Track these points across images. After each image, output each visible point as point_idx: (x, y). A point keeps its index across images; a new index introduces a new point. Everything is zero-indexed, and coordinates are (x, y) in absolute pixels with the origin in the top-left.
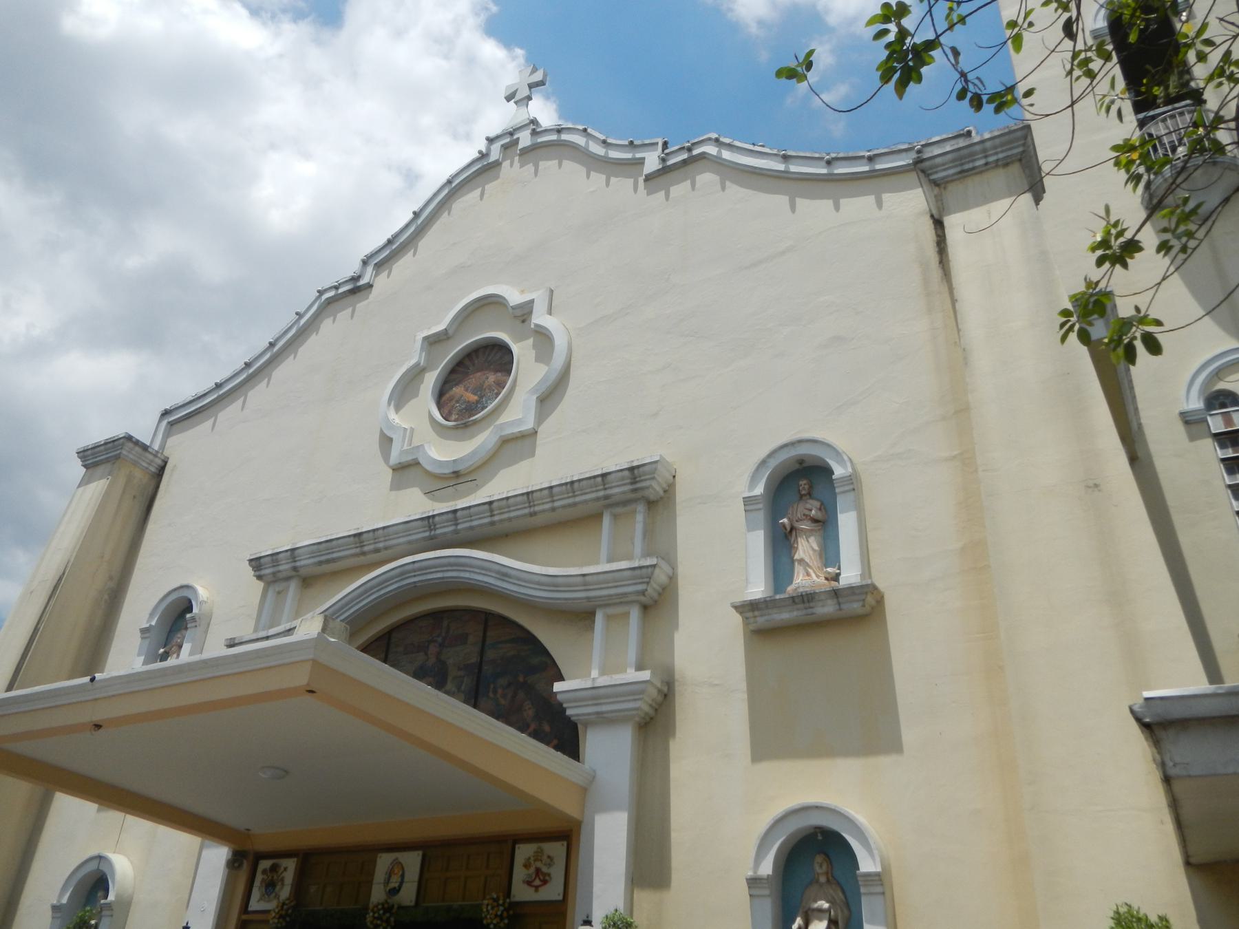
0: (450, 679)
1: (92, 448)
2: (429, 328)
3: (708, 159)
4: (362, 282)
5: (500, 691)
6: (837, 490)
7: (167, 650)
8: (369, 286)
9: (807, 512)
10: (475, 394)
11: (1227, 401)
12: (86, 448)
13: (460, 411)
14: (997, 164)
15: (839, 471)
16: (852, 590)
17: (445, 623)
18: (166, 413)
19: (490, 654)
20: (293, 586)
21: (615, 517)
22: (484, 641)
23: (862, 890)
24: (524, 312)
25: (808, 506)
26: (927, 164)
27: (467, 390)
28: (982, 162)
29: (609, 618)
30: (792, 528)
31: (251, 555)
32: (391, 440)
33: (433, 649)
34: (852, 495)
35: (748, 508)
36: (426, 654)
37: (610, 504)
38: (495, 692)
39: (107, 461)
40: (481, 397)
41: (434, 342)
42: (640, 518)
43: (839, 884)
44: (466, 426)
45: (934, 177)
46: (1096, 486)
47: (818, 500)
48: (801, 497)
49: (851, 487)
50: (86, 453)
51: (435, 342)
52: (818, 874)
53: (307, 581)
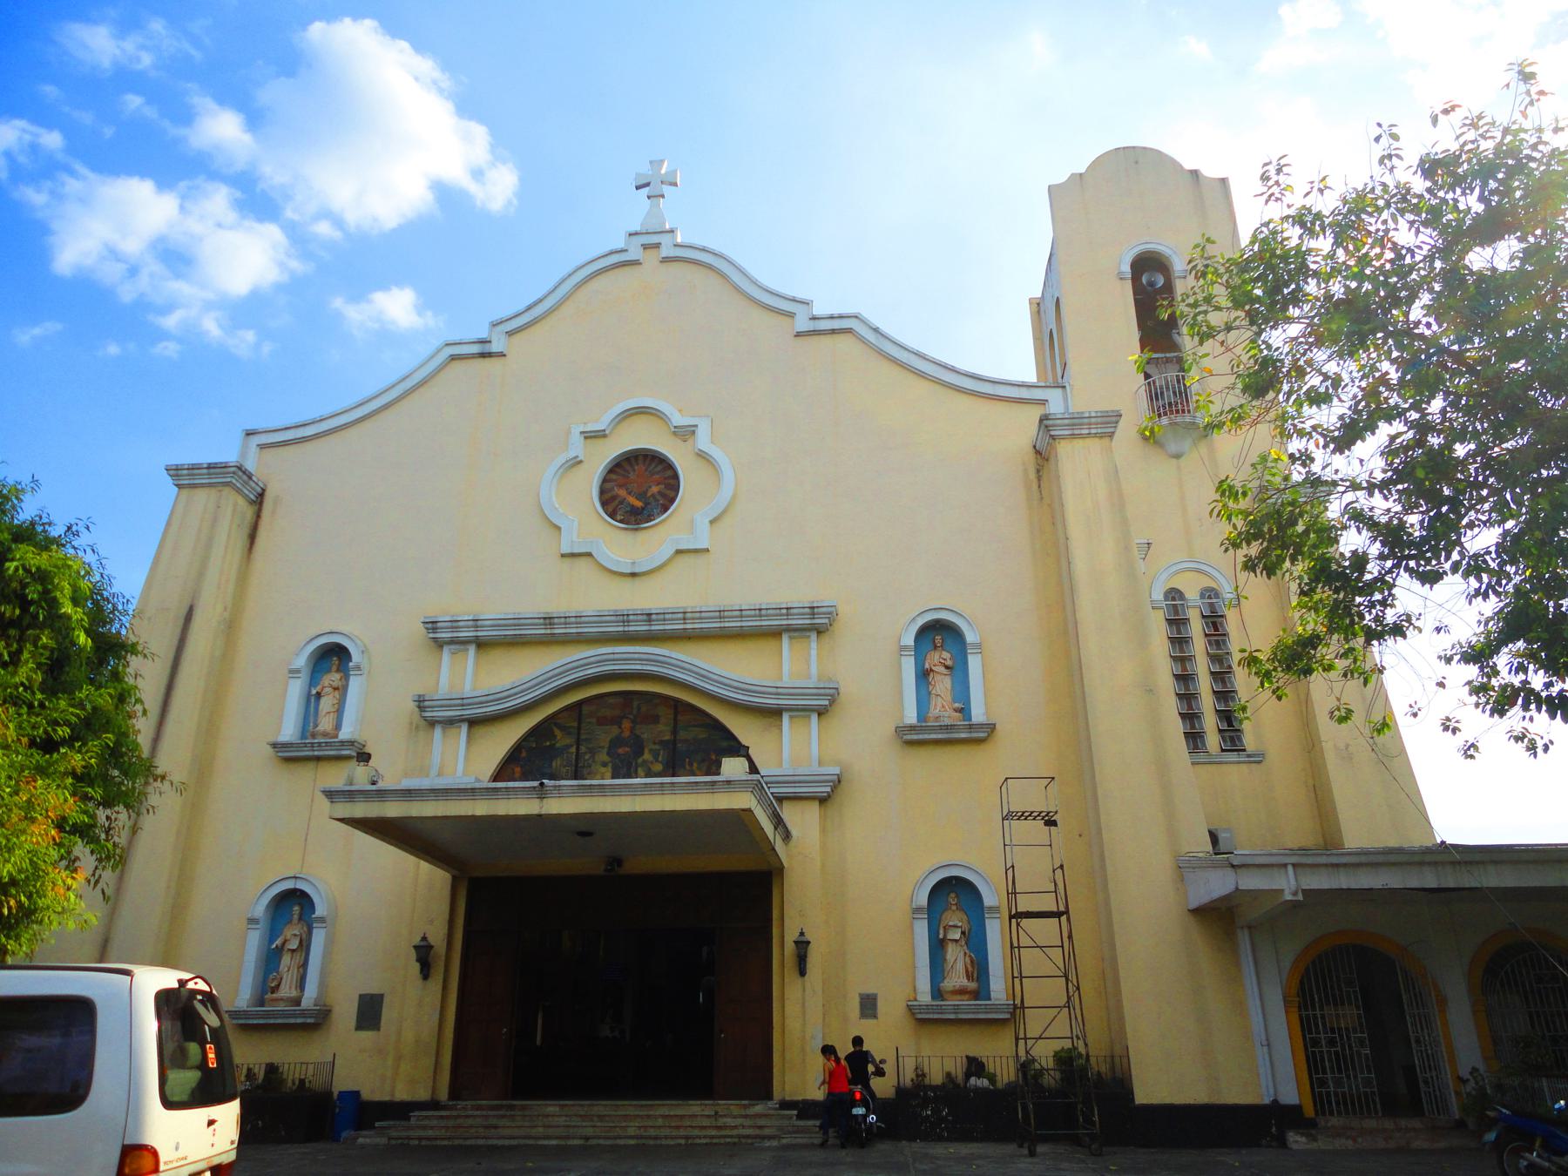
0: (646, 751)
1: (188, 469)
2: (585, 423)
4: (495, 347)
5: (695, 765)
6: (969, 651)
8: (502, 355)
9: (943, 661)
10: (640, 500)
12: (179, 467)
13: (627, 512)
15: (970, 637)
16: (981, 726)
17: (635, 704)
18: (249, 434)
19: (682, 735)
20: (472, 649)
21: (790, 638)
23: (986, 916)
24: (686, 433)
26: (1051, 422)
27: (630, 494)
28: (1086, 431)
29: (791, 717)
30: (931, 670)
31: (425, 618)
32: (559, 528)
33: (626, 724)
34: (980, 655)
35: (902, 653)
36: (620, 727)
37: (789, 629)
38: (691, 764)
39: (210, 485)
40: (647, 504)
41: (590, 436)
42: (814, 645)
43: (963, 910)
44: (636, 529)
45: (1052, 433)
46: (1151, 690)
48: (935, 647)
49: (980, 651)
50: (180, 472)
51: (591, 437)
53: (482, 644)
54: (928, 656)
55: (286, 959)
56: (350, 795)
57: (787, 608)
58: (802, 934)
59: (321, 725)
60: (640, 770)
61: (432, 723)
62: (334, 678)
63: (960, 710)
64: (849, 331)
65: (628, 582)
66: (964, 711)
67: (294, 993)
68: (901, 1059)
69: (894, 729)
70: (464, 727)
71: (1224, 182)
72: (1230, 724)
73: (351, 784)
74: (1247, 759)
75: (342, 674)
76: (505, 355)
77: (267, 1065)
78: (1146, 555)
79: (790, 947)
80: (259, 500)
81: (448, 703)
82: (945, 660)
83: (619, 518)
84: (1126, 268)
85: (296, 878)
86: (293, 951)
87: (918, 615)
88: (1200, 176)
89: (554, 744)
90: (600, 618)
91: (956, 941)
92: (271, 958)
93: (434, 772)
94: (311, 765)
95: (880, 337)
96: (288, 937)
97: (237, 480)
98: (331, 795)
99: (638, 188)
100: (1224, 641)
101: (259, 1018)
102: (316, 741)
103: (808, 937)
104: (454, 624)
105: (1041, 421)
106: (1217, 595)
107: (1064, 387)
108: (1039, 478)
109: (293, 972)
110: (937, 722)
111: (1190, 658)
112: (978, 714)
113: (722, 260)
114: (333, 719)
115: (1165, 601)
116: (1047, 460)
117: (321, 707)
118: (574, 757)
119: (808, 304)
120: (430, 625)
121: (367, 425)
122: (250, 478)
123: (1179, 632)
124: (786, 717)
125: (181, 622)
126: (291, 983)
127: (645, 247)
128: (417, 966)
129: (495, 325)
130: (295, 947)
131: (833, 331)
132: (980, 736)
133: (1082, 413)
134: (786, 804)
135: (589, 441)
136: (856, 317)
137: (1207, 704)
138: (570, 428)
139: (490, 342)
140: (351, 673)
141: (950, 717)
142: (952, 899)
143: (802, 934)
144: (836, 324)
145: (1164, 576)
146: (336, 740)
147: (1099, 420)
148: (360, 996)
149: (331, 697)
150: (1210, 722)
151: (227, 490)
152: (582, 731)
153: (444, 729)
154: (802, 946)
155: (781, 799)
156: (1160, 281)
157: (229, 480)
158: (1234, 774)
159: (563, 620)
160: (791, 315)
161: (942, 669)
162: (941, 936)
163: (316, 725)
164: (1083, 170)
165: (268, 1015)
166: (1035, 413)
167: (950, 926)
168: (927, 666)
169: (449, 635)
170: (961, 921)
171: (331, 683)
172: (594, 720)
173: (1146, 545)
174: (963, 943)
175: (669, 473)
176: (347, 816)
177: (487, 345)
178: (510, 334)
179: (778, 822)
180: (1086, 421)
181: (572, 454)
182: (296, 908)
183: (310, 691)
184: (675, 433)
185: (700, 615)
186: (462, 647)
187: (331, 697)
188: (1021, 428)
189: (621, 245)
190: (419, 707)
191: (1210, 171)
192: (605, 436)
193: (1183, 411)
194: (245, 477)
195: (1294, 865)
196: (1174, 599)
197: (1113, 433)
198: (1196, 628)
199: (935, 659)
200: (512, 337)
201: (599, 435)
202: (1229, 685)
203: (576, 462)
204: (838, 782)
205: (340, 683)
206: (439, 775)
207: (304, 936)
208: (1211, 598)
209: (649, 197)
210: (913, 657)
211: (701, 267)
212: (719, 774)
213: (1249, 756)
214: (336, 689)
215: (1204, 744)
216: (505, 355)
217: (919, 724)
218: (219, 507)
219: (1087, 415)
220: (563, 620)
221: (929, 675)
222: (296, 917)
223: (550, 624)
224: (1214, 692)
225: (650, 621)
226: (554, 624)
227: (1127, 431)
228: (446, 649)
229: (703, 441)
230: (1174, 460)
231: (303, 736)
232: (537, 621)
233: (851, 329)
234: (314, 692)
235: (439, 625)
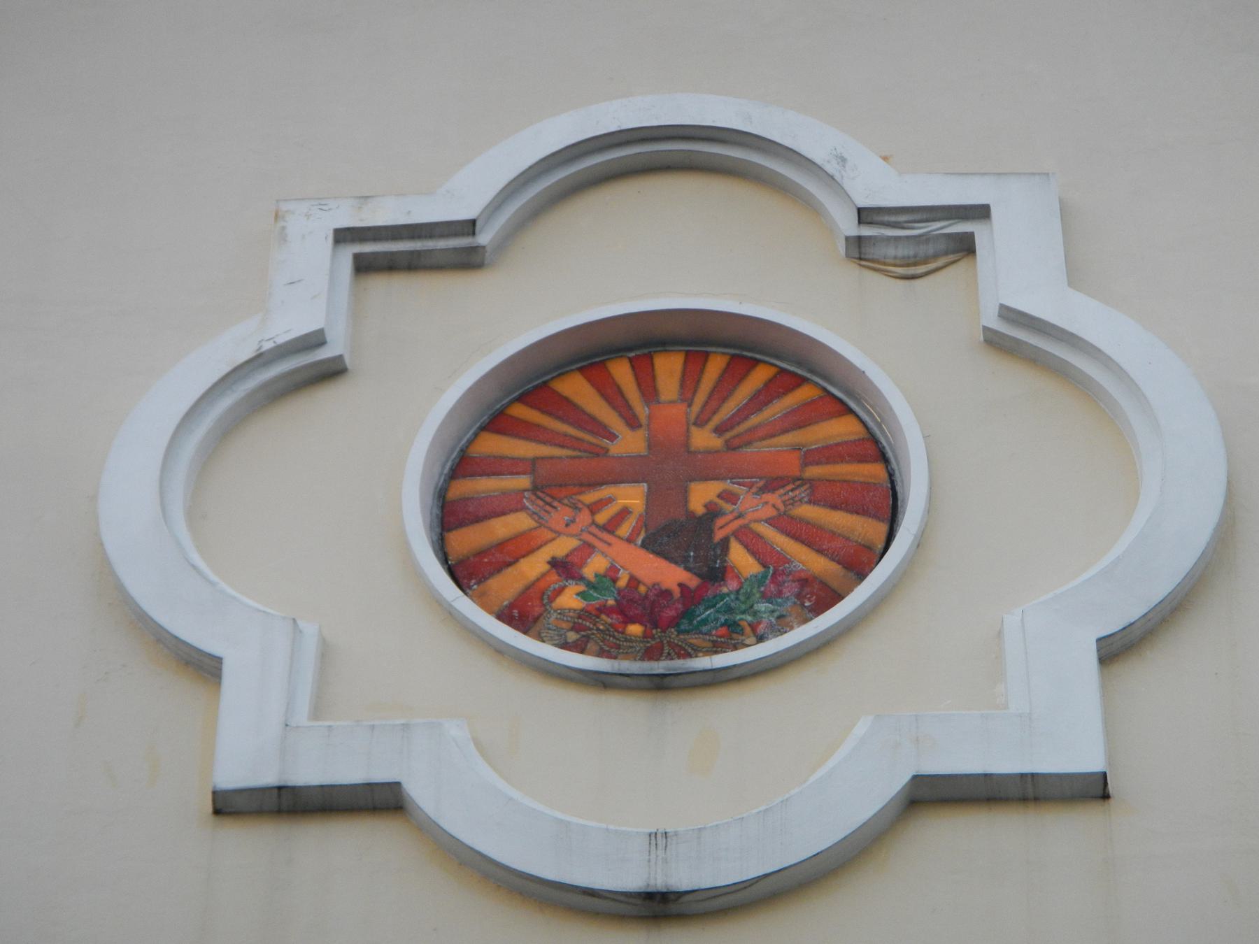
44: (660, 685)
135: (382, 286)
175: (837, 430)
184: (859, 250)
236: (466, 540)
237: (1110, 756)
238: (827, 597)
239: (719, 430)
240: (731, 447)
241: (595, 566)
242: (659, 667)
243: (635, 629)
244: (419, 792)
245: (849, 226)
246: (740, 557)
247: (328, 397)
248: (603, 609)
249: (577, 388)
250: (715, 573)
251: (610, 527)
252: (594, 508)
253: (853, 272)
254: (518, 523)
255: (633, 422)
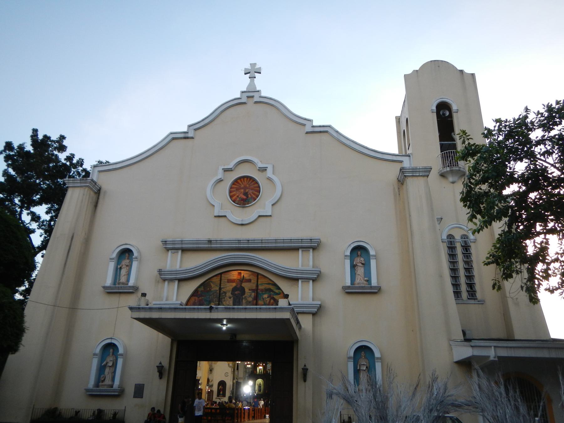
2: (224, 165)
3: (329, 133)
4: (190, 135)
7: (121, 266)
8: (192, 138)
9: (361, 261)
11: (452, 237)
14: (422, 176)
15: (372, 252)
19: (260, 287)
21: (302, 251)
22: (257, 282)
23: (376, 361)
24: (263, 170)
25: (361, 260)
26: (405, 170)
29: (302, 281)
30: (356, 264)
31: (162, 239)
32: (214, 206)
35: (345, 258)
37: (302, 247)
39: (81, 187)
41: (226, 170)
44: (243, 207)
45: (405, 174)
46: (441, 276)
47: (363, 258)
48: (358, 256)
49: (375, 258)
52: (362, 356)
53: (184, 250)
54: (355, 260)
55: (107, 370)
56: (139, 309)
57: (301, 239)
58: (305, 366)
59: (121, 280)
60: (244, 301)
61: (164, 280)
62: (126, 262)
63: (367, 281)
64: (326, 132)
65: (240, 227)
66: (369, 281)
67: (110, 383)
68: (342, 416)
69: (341, 287)
70: (177, 282)
71: (473, 75)
72: (471, 288)
73: (139, 305)
74: (478, 302)
75: (129, 260)
76: (193, 138)
77: (98, 410)
78: (440, 223)
79: (300, 370)
80: (98, 192)
81: (171, 272)
82: (362, 261)
83: (236, 202)
84: (434, 108)
85: (111, 338)
86: (110, 366)
87: (351, 244)
88: (464, 72)
89: (211, 289)
90: (229, 242)
91: (364, 370)
92: (101, 369)
93: (165, 299)
94: (118, 295)
95: (339, 134)
96: (108, 361)
97: (91, 185)
98: (131, 309)
99: (245, 74)
100: (470, 256)
101: (97, 392)
102: (120, 286)
103: (308, 367)
104: (174, 242)
105: (401, 170)
106: (467, 238)
107: (410, 156)
108: (399, 191)
109: (110, 376)
110: (358, 285)
111: (456, 262)
112: (374, 282)
113: (278, 103)
114: (126, 278)
115: (447, 239)
116: (403, 184)
117: (121, 273)
118: (218, 295)
119: (311, 121)
120: (164, 242)
121: (141, 164)
122: (96, 184)
123: (454, 266)
124: (300, 281)
125: (70, 239)
126: (109, 379)
127: (248, 97)
128: (158, 374)
129: (190, 126)
130: (111, 365)
131: (320, 132)
132: (376, 291)
133: (417, 167)
134: (299, 314)
135: (225, 172)
136: (329, 126)
137: (463, 280)
138: (218, 167)
139: (188, 133)
140: (134, 260)
141: (365, 284)
142: (363, 354)
143: (305, 366)
144: (322, 129)
145: (447, 229)
146: (128, 286)
147: (423, 170)
148: (135, 384)
149: (125, 269)
150: (464, 288)
151: (87, 188)
152: (222, 285)
153: (168, 282)
154: (305, 371)
155: (298, 313)
156: (447, 113)
157: (88, 185)
158: (473, 308)
159: (215, 242)
160: (304, 125)
161: (360, 264)
162: (358, 368)
163: (119, 280)
164: (418, 69)
165: (101, 391)
166: (398, 166)
167: (362, 364)
168: (355, 263)
169: (171, 246)
170: (366, 363)
171: (126, 263)
172: (226, 281)
173: (440, 219)
174: (367, 371)
175: (256, 185)
176: (137, 317)
177: (187, 134)
178: (195, 130)
179: (298, 322)
180: (418, 170)
181: (219, 177)
182: (111, 350)
183: (117, 266)
184: (259, 170)
185: (268, 241)
186: (176, 251)
187: (125, 269)
188: (393, 171)
189: (238, 96)
190: (160, 274)
191: (468, 70)
192: (232, 170)
193: (456, 165)
194: (94, 184)
195: (495, 347)
196: (450, 239)
197: (429, 175)
198: (459, 250)
199: (359, 260)
200: (197, 131)
201: (230, 170)
202: (471, 273)
203: (220, 181)
204: (320, 308)
205: (129, 264)
206: (166, 300)
207: (114, 361)
208: (465, 239)
209: (250, 78)
210: (349, 260)
211: (269, 105)
212: (277, 305)
213: (479, 301)
214: (127, 266)
215: (461, 296)
216: (193, 138)
217: (351, 286)
218: (84, 195)
219: (418, 168)
220: (215, 242)
221: (355, 266)
222: (111, 354)
223: (210, 243)
224: (466, 276)
225: (248, 243)
226: (212, 243)
227: (434, 174)
228: (170, 252)
229: (269, 173)
230: (452, 184)
231: (114, 284)
232: (205, 242)
233: (327, 131)
234: (119, 267)
235: (167, 242)
236: (232, 194)
237: (272, 214)
238: (255, 200)
239: (249, 185)
240: (249, 186)
241: (240, 196)
242: (243, 206)
243: (242, 202)
244: (227, 216)
245: (258, 168)
246: (249, 196)
247: (222, 183)
248: (240, 200)
249: (239, 181)
250: (248, 197)
251: (241, 193)
252: (240, 191)
253: (258, 172)
254: (235, 193)
255: (243, 184)
